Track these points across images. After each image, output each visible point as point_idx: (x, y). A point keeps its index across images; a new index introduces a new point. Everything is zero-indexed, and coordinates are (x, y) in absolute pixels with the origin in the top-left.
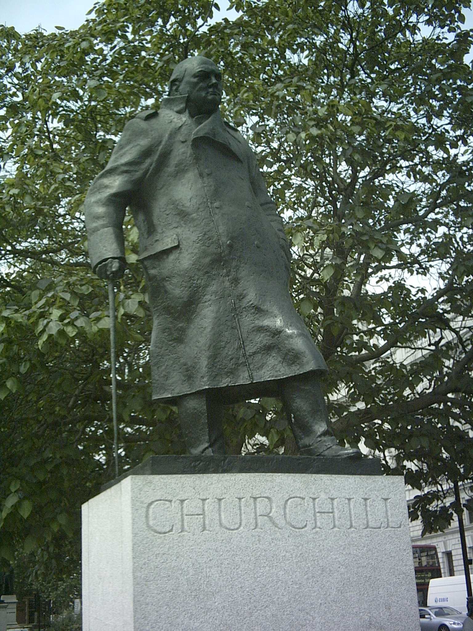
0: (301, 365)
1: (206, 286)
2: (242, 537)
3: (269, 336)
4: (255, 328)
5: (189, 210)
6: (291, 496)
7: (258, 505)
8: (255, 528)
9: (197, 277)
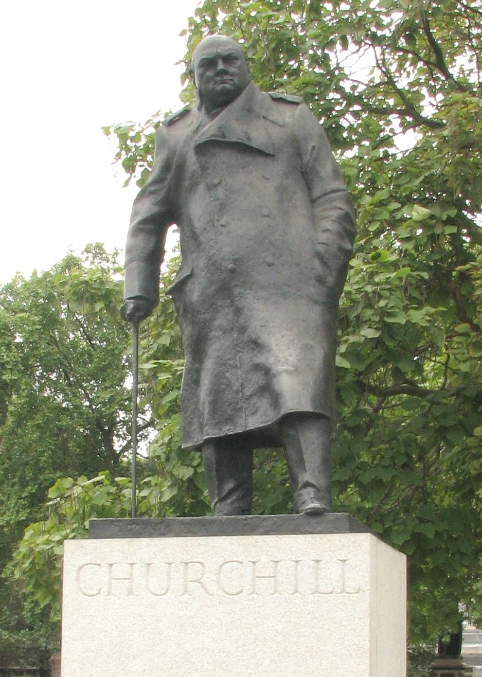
6: (226, 561)
8: (184, 594)
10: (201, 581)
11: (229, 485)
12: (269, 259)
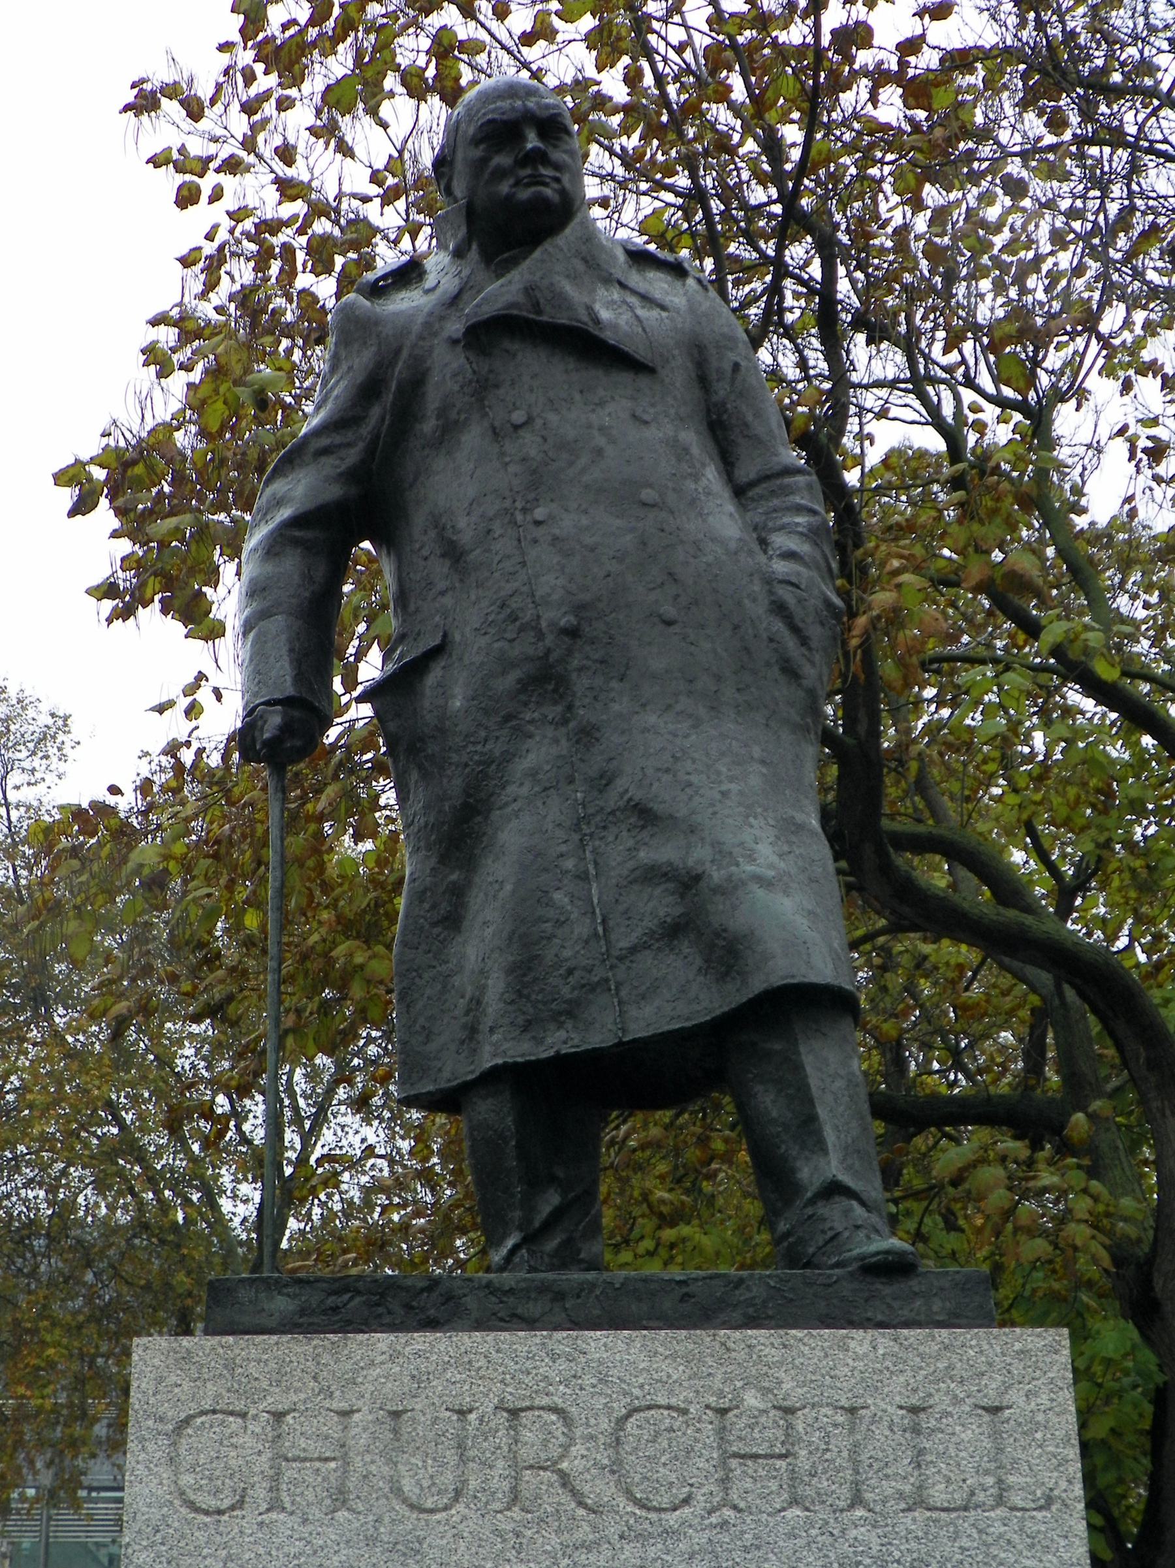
2: (458, 1536)
3: (673, 894)
4: (638, 873)
7: (527, 1435)
9: (483, 734)
10: (564, 1465)
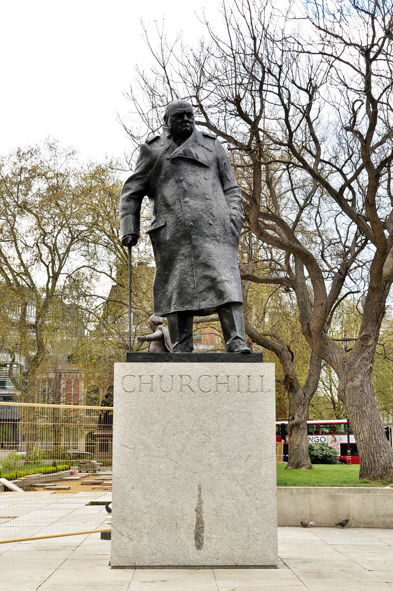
0: (223, 299)
1: (180, 250)
5: (170, 203)
7: (183, 380)
11: (184, 336)
12: (211, 222)
